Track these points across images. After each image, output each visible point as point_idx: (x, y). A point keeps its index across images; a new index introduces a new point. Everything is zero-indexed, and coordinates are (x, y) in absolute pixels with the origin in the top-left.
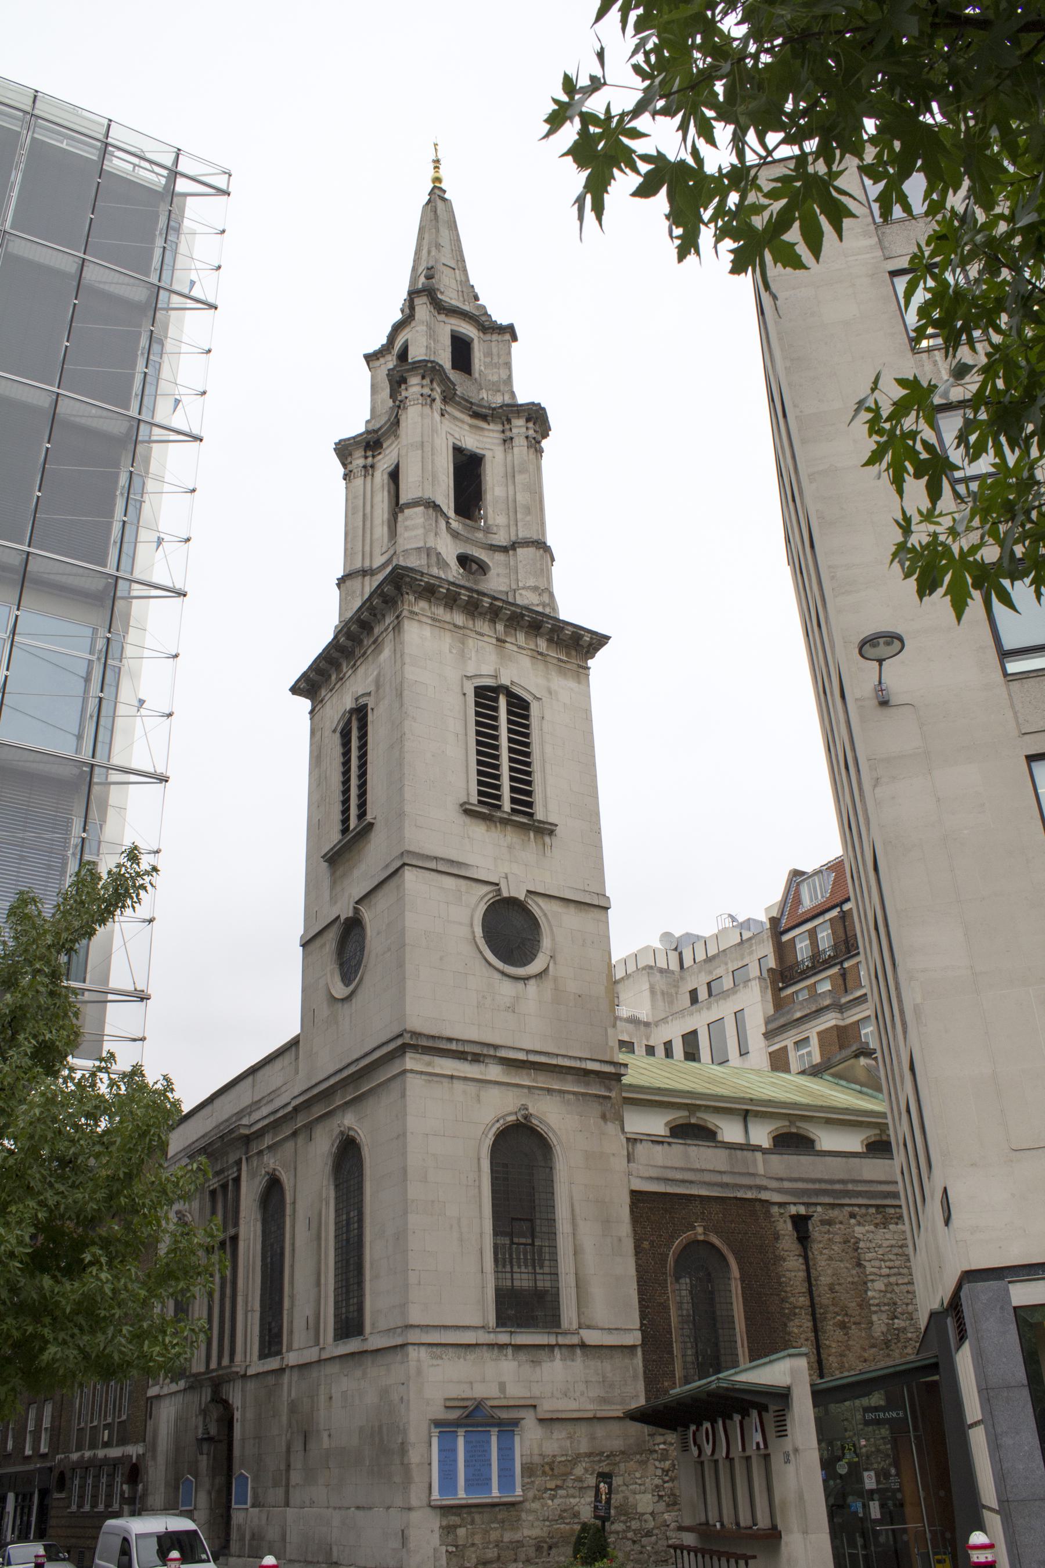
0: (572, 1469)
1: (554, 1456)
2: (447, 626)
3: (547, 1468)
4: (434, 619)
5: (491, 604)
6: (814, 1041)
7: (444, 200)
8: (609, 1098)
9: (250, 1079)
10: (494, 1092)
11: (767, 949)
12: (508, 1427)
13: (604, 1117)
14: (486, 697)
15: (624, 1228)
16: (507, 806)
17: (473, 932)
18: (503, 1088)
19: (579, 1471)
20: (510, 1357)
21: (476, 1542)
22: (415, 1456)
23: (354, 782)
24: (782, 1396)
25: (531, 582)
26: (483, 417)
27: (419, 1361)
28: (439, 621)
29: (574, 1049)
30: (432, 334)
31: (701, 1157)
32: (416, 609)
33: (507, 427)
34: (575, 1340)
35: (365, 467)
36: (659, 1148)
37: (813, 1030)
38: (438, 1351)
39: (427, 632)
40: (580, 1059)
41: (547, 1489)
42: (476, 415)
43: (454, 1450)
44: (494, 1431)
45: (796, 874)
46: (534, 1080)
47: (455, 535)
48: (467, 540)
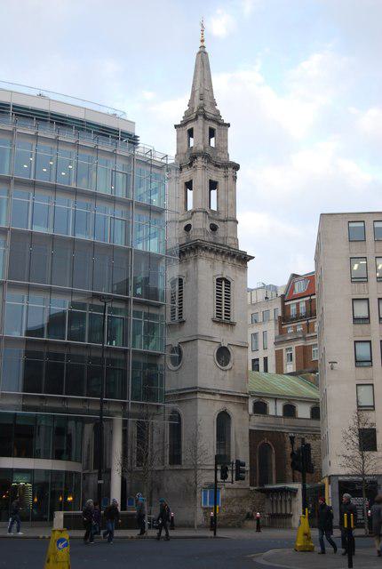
6: (294, 350)
7: (205, 53)
10: (218, 403)
11: (278, 306)
14: (219, 280)
15: (247, 440)
16: (223, 317)
24: (297, 490)
25: (232, 235)
26: (218, 166)
29: (238, 391)
31: (267, 420)
37: (294, 346)
42: (216, 166)
45: (294, 276)
48: (212, 218)
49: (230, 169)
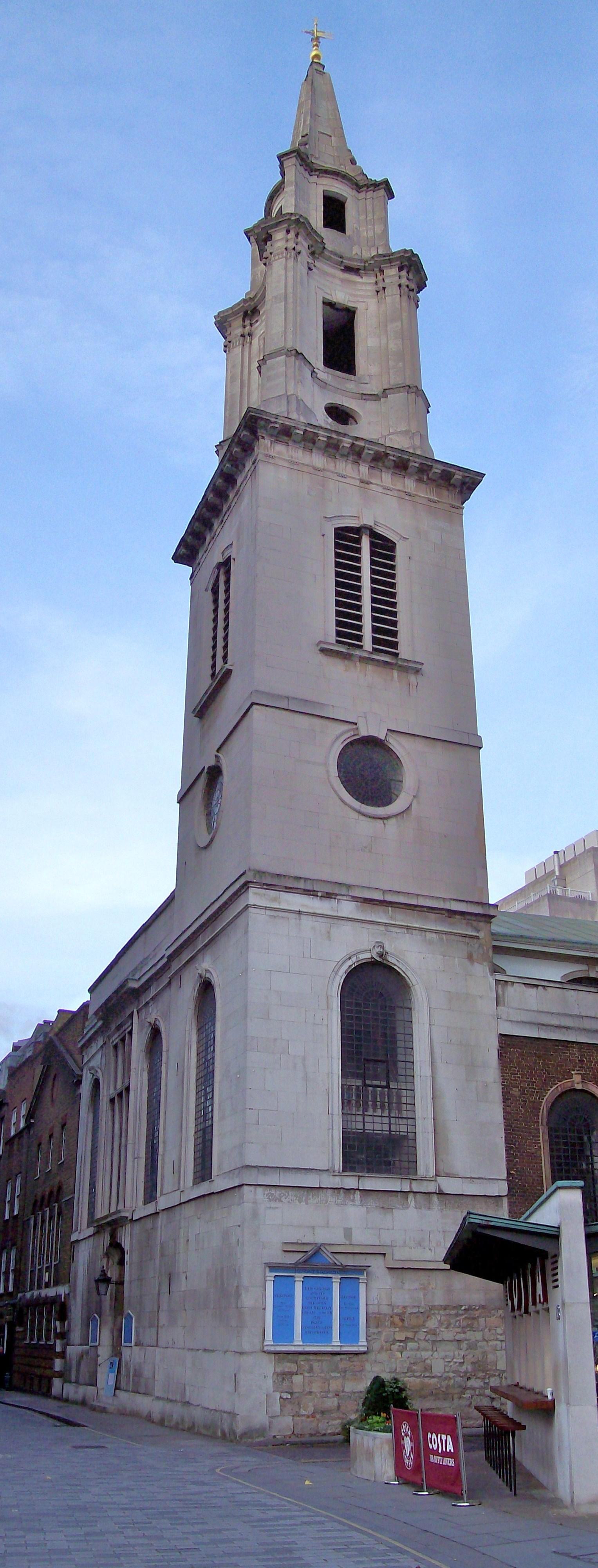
0: (424, 1321)
1: (405, 1307)
2: (305, 469)
3: (397, 1319)
4: (291, 462)
5: (353, 444)
8: (477, 938)
9: (143, 936)
12: (351, 1274)
13: (470, 957)
17: (328, 772)
18: (357, 924)
19: (432, 1323)
20: (358, 1202)
21: (313, 1390)
22: (248, 1300)
23: (221, 634)
26: (356, 271)
27: (255, 1202)
28: (297, 464)
30: (301, 195)
32: (272, 453)
33: (380, 278)
34: (431, 1187)
35: (243, 336)
36: (533, 991)
38: (276, 1193)
39: (284, 475)
40: (444, 899)
41: (395, 1341)
42: (348, 269)
43: (292, 1296)
44: (336, 1279)
46: (391, 918)
47: (323, 385)
49: (392, 272)
